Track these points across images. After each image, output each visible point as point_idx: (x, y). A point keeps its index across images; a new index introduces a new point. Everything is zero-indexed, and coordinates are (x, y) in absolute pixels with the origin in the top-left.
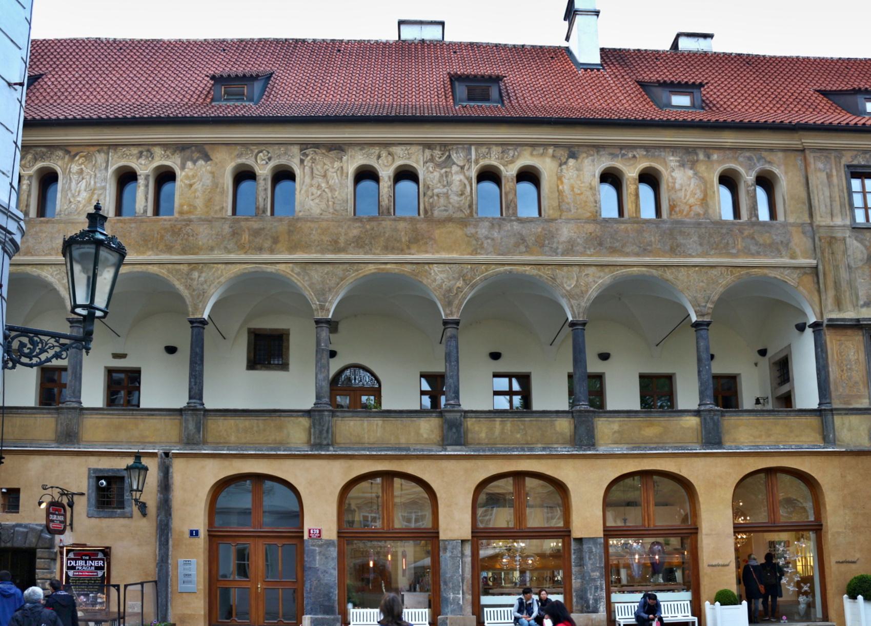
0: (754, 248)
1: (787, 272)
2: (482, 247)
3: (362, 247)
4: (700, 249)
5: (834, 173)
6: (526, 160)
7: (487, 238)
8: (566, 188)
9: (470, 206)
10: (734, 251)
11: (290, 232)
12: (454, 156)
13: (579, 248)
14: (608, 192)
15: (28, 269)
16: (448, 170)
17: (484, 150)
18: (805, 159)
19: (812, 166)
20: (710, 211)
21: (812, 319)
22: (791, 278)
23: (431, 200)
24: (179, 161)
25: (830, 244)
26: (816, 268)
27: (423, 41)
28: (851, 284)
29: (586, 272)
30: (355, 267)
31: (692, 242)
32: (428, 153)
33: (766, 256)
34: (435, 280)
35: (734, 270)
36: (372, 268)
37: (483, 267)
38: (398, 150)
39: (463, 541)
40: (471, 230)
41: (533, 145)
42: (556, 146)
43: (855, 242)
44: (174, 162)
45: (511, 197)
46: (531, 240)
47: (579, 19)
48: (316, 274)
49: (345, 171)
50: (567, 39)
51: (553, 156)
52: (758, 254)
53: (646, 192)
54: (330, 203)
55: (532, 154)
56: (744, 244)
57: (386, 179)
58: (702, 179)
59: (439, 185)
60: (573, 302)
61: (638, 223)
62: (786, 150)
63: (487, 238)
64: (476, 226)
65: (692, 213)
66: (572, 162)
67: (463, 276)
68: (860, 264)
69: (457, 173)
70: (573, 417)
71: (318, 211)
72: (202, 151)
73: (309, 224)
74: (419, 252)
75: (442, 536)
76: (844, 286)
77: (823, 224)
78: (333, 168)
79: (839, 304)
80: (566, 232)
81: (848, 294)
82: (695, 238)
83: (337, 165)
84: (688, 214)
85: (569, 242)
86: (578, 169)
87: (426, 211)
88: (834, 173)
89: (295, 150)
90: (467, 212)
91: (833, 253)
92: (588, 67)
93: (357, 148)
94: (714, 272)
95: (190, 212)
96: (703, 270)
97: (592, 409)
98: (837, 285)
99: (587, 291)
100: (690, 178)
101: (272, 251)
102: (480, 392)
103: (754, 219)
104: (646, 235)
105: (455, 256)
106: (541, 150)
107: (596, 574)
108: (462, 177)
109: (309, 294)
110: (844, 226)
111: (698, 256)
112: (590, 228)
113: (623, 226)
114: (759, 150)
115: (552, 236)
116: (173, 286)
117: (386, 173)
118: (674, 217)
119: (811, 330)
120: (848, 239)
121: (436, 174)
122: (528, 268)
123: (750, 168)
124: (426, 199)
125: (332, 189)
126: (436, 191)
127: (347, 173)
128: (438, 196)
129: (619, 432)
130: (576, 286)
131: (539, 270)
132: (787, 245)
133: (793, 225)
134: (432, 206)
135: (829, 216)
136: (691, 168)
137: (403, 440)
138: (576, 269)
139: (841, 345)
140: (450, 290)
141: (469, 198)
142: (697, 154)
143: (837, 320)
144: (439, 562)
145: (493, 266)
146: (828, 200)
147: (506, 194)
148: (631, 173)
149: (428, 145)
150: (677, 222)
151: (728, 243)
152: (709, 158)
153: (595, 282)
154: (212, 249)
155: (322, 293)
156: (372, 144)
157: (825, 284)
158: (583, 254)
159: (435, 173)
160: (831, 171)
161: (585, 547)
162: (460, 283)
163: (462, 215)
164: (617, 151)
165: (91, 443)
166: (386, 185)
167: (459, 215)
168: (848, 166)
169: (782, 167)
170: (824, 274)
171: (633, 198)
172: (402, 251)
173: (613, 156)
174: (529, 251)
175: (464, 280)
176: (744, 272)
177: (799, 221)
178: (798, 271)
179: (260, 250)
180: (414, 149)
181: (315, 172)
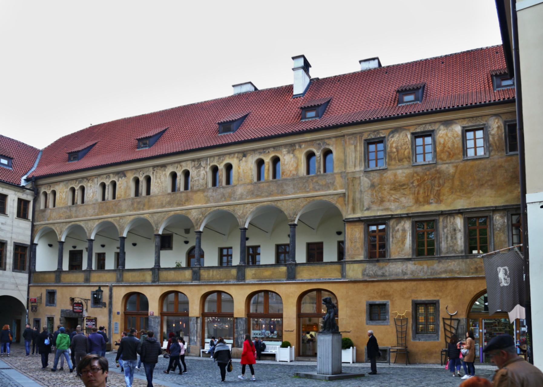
0: (317, 187)
1: (332, 197)
2: (209, 200)
4: (293, 191)
5: (358, 145)
7: (211, 196)
8: (241, 171)
9: (206, 184)
10: (308, 190)
11: (149, 202)
13: (244, 197)
15: (78, 223)
17: (212, 159)
19: (348, 143)
20: (299, 172)
24: (117, 178)
25: (352, 181)
28: (361, 200)
31: (289, 188)
32: (193, 163)
33: (323, 190)
35: (307, 199)
36: (172, 213)
40: (206, 194)
41: (230, 154)
42: (238, 152)
44: (115, 179)
45: (221, 177)
46: (227, 195)
48: (156, 217)
52: (319, 190)
60: (241, 220)
61: (268, 182)
62: (336, 137)
63: (211, 196)
64: (207, 192)
65: (291, 175)
66: (244, 158)
67: (202, 213)
68: (367, 189)
71: (157, 192)
72: (122, 174)
73: (155, 198)
74: (188, 205)
75: (190, 315)
76: (357, 201)
77: (350, 171)
79: (354, 210)
81: (359, 205)
82: (292, 186)
84: (289, 175)
86: (246, 162)
87: (191, 188)
88: (358, 145)
90: (205, 186)
91: (353, 185)
94: (298, 201)
95: (120, 197)
96: (294, 200)
98: (354, 201)
100: (291, 158)
101: (143, 209)
104: (271, 187)
105: (199, 205)
106: (232, 155)
107: (242, 332)
109: (153, 225)
110: (361, 171)
111: (293, 194)
112: (249, 187)
114: (324, 139)
115: (234, 192)
120: (362, 178)
121: (196, 172)
122: (225, 207)
125: (162, 183)
133: (336, 174)
134: (193, 185)
135: (353, 167)
136: (292, 153)
137: (180, 279)
138: (242, 206)
139: (352, 230)
140: (197, 219)
142: (295, 146)
146: (354, 159)
151: (306, 187)
154: (126, 210)
155: (157, 225)
156: (175, 163)
157: (348, 201)
158: (246, 199)
160: (357, 143)
162: (201, 216)
164: (262, 151)
165: (93, 282)
167: (202, 188)
168: (365, 140)
169: (334, 146)
170: (348, 196)
172: (183, 205)
173: (260, 153)
174: (225, 201)
176: (311, 199)
177: (340, 171)
178: (337, 196)
179: (139, 209)
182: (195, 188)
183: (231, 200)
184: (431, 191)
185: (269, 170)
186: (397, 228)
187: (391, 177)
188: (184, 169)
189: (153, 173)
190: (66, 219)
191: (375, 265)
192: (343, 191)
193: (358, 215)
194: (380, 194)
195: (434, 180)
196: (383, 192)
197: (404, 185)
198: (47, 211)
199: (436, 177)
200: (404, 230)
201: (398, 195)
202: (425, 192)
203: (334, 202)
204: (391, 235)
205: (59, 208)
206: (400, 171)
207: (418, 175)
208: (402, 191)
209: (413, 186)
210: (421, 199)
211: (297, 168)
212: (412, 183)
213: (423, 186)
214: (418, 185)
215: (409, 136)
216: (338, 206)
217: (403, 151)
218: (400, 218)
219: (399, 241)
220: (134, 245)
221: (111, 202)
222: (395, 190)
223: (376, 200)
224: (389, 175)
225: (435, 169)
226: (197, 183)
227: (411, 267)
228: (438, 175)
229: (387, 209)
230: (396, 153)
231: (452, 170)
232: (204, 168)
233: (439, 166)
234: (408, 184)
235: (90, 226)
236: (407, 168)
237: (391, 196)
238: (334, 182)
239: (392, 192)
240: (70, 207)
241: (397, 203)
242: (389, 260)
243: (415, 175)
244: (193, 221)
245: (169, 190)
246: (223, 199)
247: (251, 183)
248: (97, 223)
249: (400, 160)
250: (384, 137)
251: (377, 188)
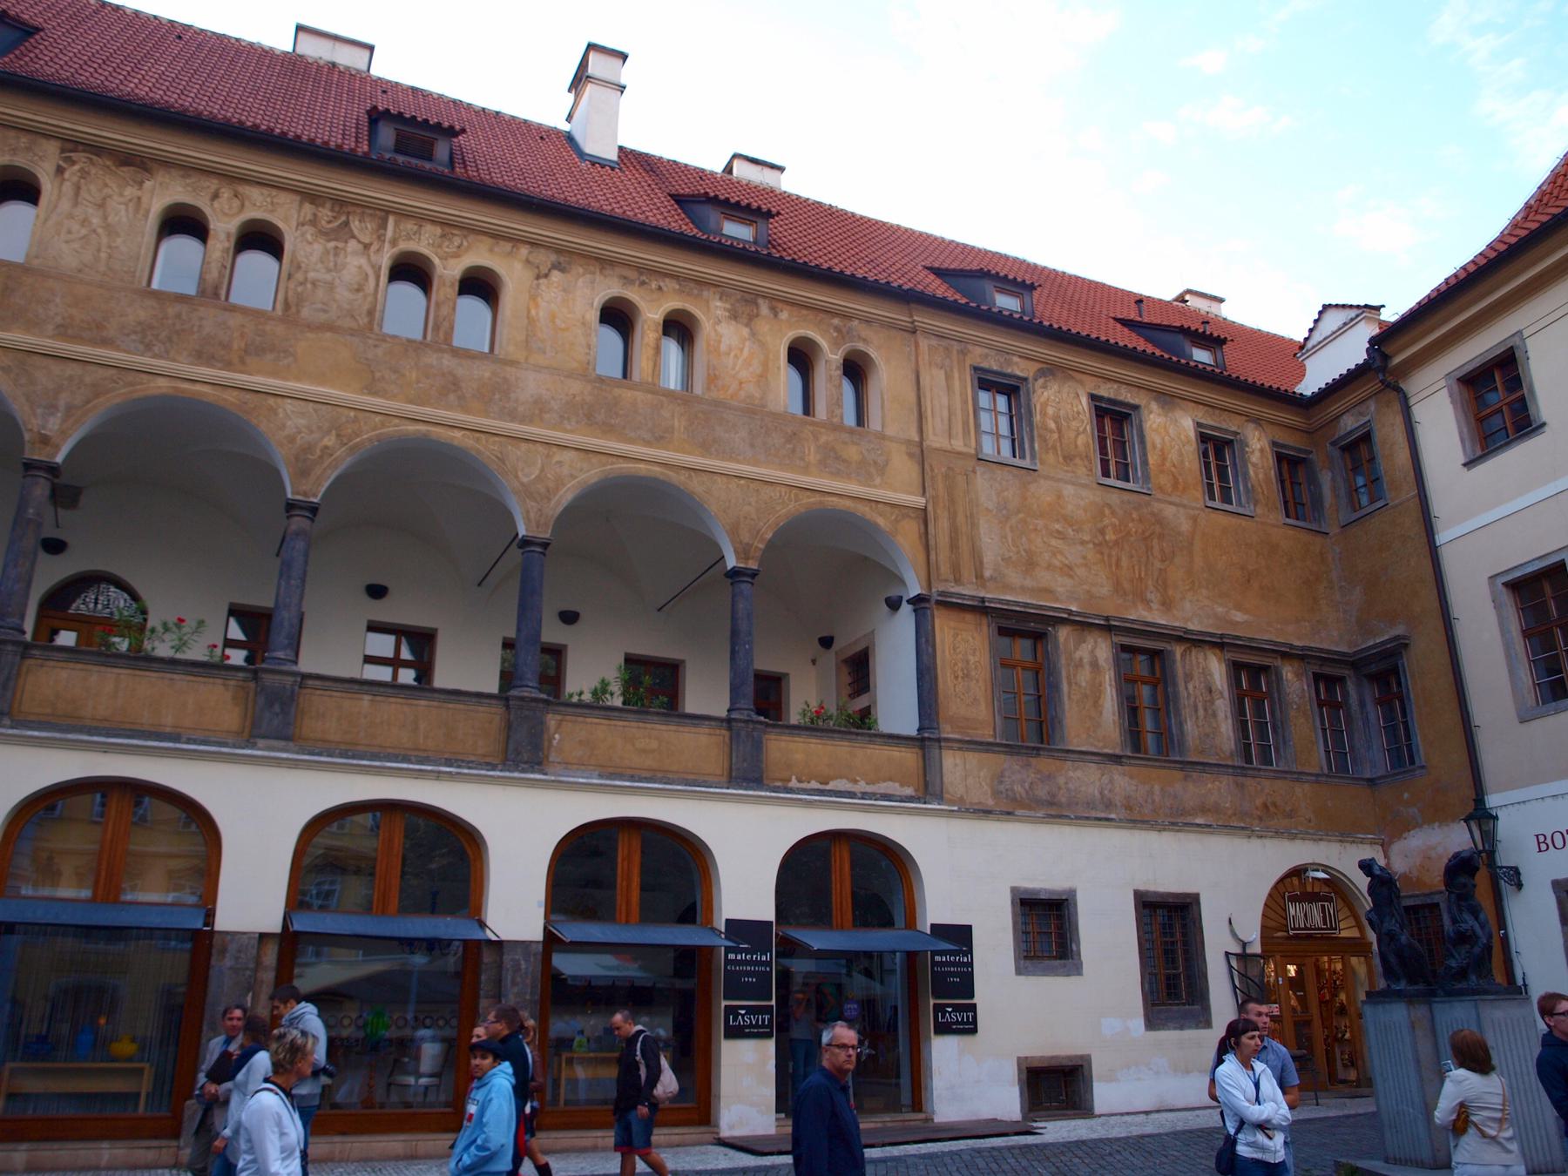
3: (148, 347)
5: (956, 375)
6: (480, 256)
9: (371, 313)
12: (355, 225)
14: (610, 339)
16: (340, 245)
17: (410, 226)
18: (917, 345)
21: (915, 589)
23: (300, 289)
26: (925, 510)
27: (334, 65)
29: (557, 458)
30: (130, 377)
32: (308, 209)
34: (283, 427)
36: (162, 384)
37: (378, 419)
38: (255, 193)
39: (263, 937)
41: (497, 236)
45: (444, 311)
47: (590, 90)
49: (144, 205)
50: (569, 118)
51: (528, 261)
53: (672, 349)
54: (103, 255)
55: (491, 250)
57: (223, 236)
58: (762, 345)
59: (319, 266)
60: (531, 504)
61: (653, 393)
66: (556, 276)
69: (355, 253)
70: (508, 707)
78: (121, 195)
80: (531, 385)
83: (130, 192)
85: (536, 402)
87: (287, 305)
88: (956, 375)
89: (52, 148)
90: (363, 320)
92: (597, 162)
93: (174, 172)
94: (767, 492)
97: (544, 696)
99: (557, 489)
102: (339, 646)
104: (666, 414)
106: (508, 246)
108: (363, 261)
112: (576, 387)
113: (627, 395)
117: (224, 226)
118: (714, 394)
119: (910, 607)
122: (458, 434)
123: (836, 344)
124: (292, 285)
126: (311, 275)
127: (148, 211)
128: (314, 284)
130: (538, 477)
131: (478, 440)
133: (891, 439)
134: (301, 299)
136: (747, 325)
138: (540, 448)
140: (308, 448)
141: (370, 299)
142: (757, 305)
143: (952, 595)
144: (206, 979)
145: (397, 421)
146: (945, 413)
147: (438, 305)
148: (651, 313)
149: (310, 196)
150: (717, 403)
152: (776, 315)
153: (573, 477)
159: (316, 246)
161: (506, 958)
163: (353, 325)
166: (219, 246)
167: (347, 323)
168: (976, 369)
171: (651, 352)
172: (228, 365)
173: (627, 281)
175: (338, 436)
180: (283, 198)
181: (84, 194)
183: (487, 415)
186: (1078, 655)
188: (252, 214)
189: (60, 171)
191: (1029, 765)
192: (920, 501)
196: (1033, 536)
200: (1095, 665)
204: (1064, 674)
206: (1068, 490)
207: (1113, 513)
210: (1127, 586)
211: (763, 378)
214: (1116, 543)
215: (1084, 400)
217: (1072, 435)
218: (1083, 625)
219: (1086, 696)
224: (1042, 491)
227: (1122, 782)
228: (1158, 529)
230: (1056, 436)
231: (1185, 526)
236: (1085, 486)
237: (1054, 555)
242: (1068, 751)
243: (1107, 511)
249: (1068, 459)
250: (1025, 379)
251: (1013, 521)
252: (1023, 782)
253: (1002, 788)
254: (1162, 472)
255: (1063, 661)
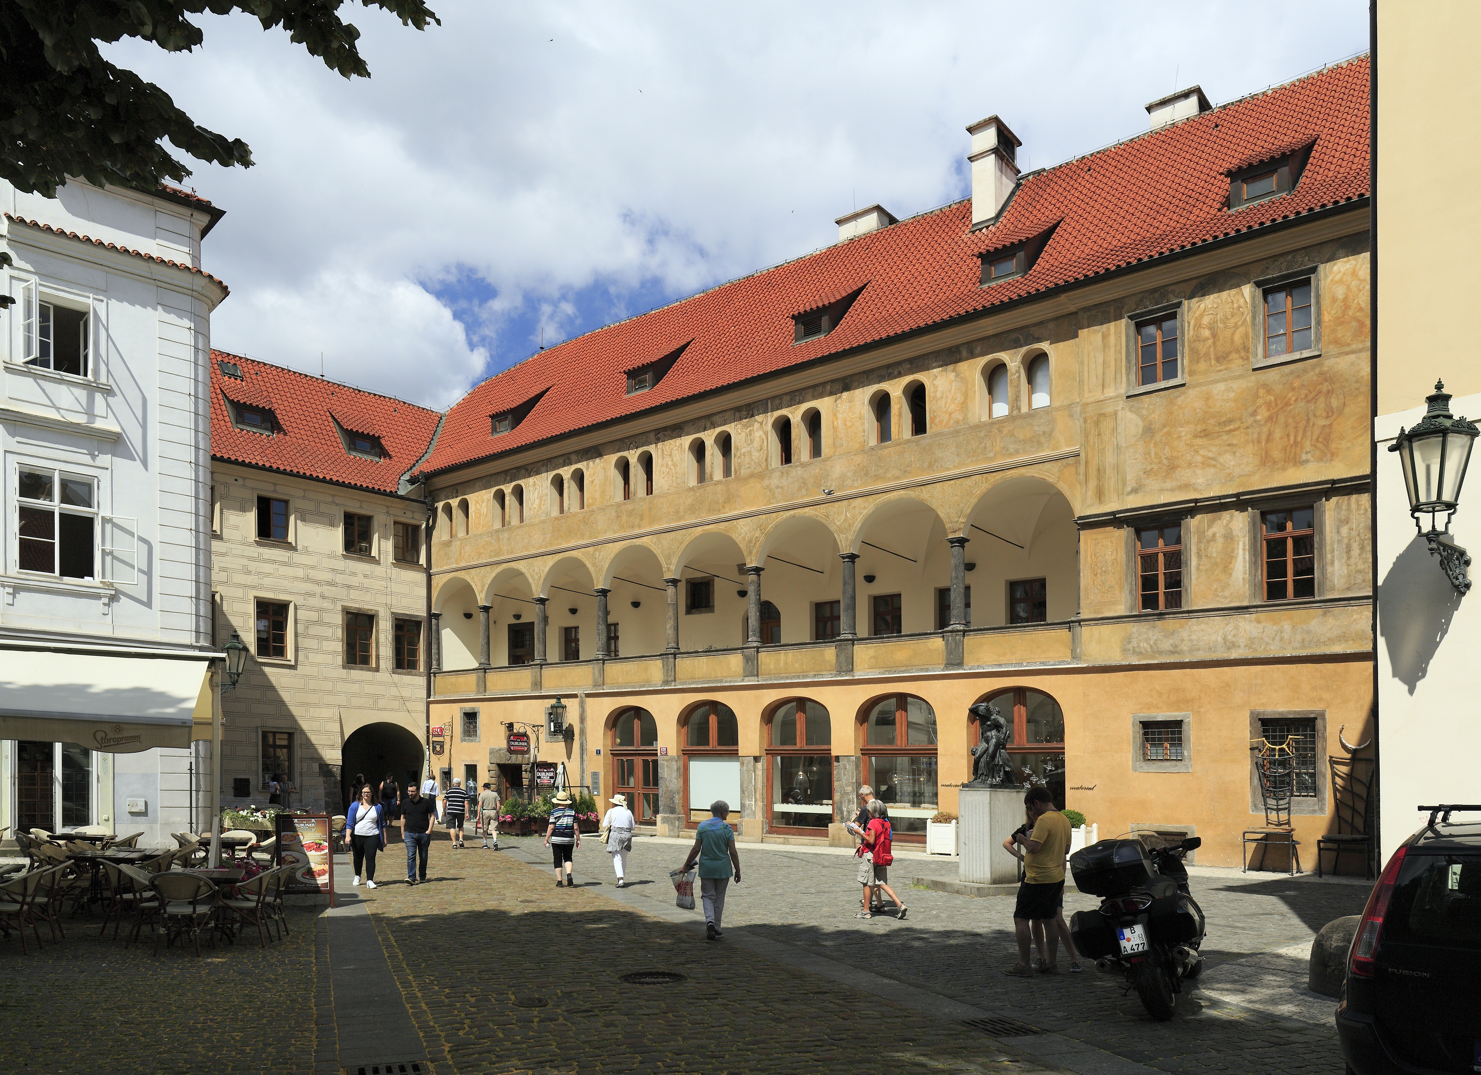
0: (1012, 447)
7: (778, 487)
8: (839, 423)
10: (992, 455)
13: (848, 482)
22: (1049, 474)
28: (1118, 468)
40: (766, 482)
43: (1129, 413)
52: (1017, 452)
56: (1002, 445)
60: (842, 536)
63: (778, 487)
65: (952, 421)
79: (1100, 495)
91: (1099, 434)
96: (958, 482)
98: (1100, 472)
101: (639, 527)
103: (1015, 413)
111: (956, 467)
112: (859, 459)
116: (585, 565)
122: (807, 509)
129: (874, 657)
130: (845, 520)
132: (1050, 435)
137: (719, 675)
138: (845, 502)
151: (985, 447)
154: (605, 532)
162: (758, 533)
182: (744, 472)
184: (1305, 431)
185: (900, 415)
187: (1196, 405)
190: (490, 557)
193: (1112, 505)
194: (1167, 449)
195: (1315, 399)
197: (1230, 421)
198: (454, 543)
199: (1320, 392)
201: (1214, 449)
202: (1288, 435)
203: (1051, 479)
205: (476, 536)
208: (1225, 437)
209: (1255, 421)
211: (964, 406)
212: (1254, 413)
213: (1282, 419)
214: (1270, 418)
216: (1063, 487)
220: (636, 605)
221: (575, 515)
222: (1206, 436)
223: (1155, 467)
225: (1317, 371)
226: (747, 460)
228: (1325, 387)
229: (1186, 487)
232: (761, 424)
233: (1328, 363)
234: (1240, 419)
235: (537, 570)
238: (1052, 431)
239: (1199, 441)
240: (497, 531)
241: (1212, 470)
244: (742, 546)
245: (693, 482)
246: (804, 492)
247: (862, 451)
248: (551, 561)
251: (1158, 437)
252: (1147, 640)
253: (1130, 647)
254: (1342, 323)
255: (1194, 540)
